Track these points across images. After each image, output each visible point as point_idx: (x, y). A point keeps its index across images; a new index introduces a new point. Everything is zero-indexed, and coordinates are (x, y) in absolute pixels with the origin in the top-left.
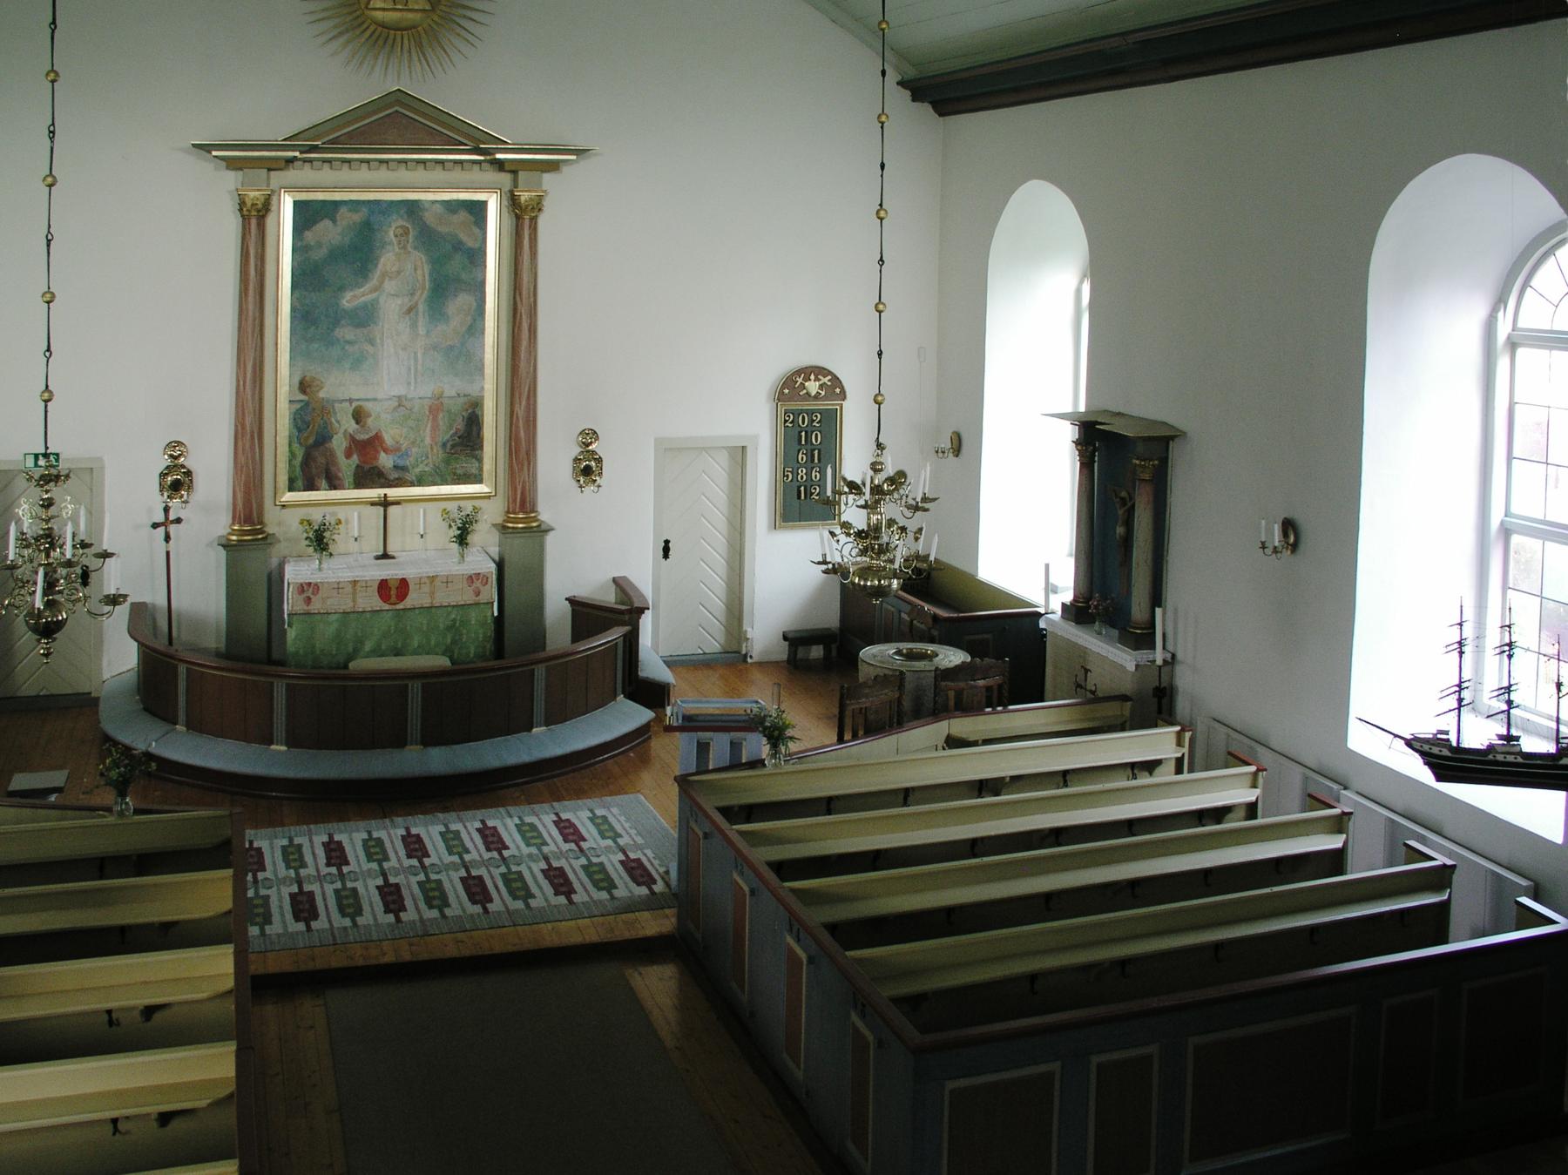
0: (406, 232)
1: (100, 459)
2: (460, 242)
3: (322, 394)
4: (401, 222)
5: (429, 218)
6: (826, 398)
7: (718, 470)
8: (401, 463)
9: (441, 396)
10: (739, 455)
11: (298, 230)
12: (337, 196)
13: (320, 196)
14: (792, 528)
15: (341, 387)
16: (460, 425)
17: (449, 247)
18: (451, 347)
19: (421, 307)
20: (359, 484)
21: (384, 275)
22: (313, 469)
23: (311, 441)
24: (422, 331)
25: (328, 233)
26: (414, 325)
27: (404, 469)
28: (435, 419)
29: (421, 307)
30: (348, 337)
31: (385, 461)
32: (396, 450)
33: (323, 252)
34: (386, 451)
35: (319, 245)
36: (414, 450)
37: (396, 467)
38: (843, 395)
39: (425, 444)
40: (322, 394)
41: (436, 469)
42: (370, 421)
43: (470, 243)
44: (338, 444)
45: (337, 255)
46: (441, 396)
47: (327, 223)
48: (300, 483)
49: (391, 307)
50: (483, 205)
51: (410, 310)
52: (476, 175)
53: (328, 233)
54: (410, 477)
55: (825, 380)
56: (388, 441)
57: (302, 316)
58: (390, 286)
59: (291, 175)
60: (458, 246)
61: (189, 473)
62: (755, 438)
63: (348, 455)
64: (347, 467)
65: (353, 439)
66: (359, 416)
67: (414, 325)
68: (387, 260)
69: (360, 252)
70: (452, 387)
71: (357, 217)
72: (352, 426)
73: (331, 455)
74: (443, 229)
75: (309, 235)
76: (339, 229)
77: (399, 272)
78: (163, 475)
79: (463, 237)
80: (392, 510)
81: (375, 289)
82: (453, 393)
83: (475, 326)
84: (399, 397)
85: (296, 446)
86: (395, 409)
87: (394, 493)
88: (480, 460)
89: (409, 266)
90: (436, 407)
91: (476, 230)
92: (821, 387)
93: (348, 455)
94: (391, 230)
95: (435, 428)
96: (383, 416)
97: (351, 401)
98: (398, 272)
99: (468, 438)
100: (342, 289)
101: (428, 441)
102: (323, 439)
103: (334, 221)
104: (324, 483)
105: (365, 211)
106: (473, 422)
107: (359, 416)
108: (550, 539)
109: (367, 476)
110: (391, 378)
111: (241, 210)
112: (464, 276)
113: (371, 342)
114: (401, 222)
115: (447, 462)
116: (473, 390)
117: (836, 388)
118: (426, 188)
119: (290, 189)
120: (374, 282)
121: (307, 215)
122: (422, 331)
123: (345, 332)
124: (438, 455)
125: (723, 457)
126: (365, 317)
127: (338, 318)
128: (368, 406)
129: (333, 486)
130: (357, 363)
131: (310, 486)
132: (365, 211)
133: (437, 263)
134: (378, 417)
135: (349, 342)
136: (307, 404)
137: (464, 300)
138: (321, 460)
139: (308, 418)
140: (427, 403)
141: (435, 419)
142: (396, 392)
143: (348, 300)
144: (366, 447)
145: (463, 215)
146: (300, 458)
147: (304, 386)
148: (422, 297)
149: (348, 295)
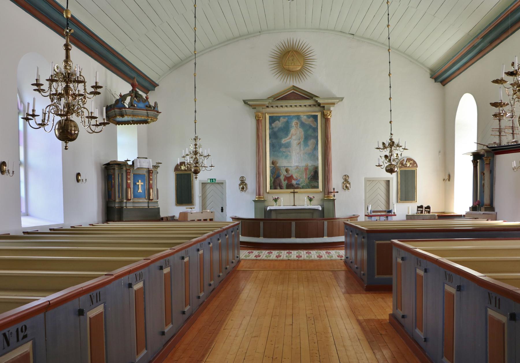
0: (297, 124)
1: (225, 181)
3: (278, 165)
8: (298, 183)
10: (388, 182)
11: (270, 124)
12: (279, 115)
13: (275, 115)
15: (283, 163)
16: (312, 173)
18: (309, 154)
19: (302, 143)
22: (276, 184)
24: (302, 149)
27: (299, 184)
28: (306, 172)
30: (284, 151)
31: (294, 182)
32: (297, 179)
34: (294, 180)
35: (276, 127)
37: (296, 184)
40: (278, 165)
41: (307, 185)
42: (290, 172)
43: (314, 126)
44: (282, 178)
45: (280, 129)
47: (277, 122)
48: (273, 187)
50: (317, 116)
51: (299, 144)
53: (278, 124)
54: (300, 186)
55: (411, 162)
56: (294, 177)
57: (272, 146)
58: (294, 137)
59: (271, 110)
60: (311, 127)
61: (246, 184)
62: (392, 178)
63: (285, 180)
64: (284, 183)
65: (285, 176)
66: (287, 171)
68: (293, 131)
69: (286, 129)
70: (310, 163)
71: (285, 120)
72: (285, 173)
73: (280, 180)
74: (307, 123)
75: (273, 125)
78: (240, 185)
79: (312, 125)
80: (296, 195)
81: (290, 138)
83: (316, 148)
84: (297, 166)
87: (296, 190)
88: (318, 182)
89: (298, 132)
90: (306, 169)
91: (315, 123)
92: (410, 164)
93: (285, 180)
94: (294, 122)
95: (306, 174)
98: (296, 134)
99: (315, 176)
100: (282, 138)
101: (304, 177)
102: (278, 176)
104: (279, 188)
105: (287, 118)
106: (316, 172)
107: (287, 171)
109: (290, 186)
110: (295, 161)
112: (312, 135)
113: (290, 152)
115: (309, 183)
116: (315, 164)
119: (268, 113)
120: (290, 136)
121: (273, 119)
122: (302, 149)
123: (283, 149)
124: (307, 181)
126: (288, 146)
127: (281, 146)
128: (289, 168)
129: (281, 188)
130: (286, 157)
131: (275, 188)
132: (287, 118)
133: (306, 131)
138: (278, 182)
140: (304, 167)
142: (296, 164)
143: (284, 141)
144: (289, 178)
145: (311, 119)
147: (273, 163)
148: (302, 141)
149: (283, 140)
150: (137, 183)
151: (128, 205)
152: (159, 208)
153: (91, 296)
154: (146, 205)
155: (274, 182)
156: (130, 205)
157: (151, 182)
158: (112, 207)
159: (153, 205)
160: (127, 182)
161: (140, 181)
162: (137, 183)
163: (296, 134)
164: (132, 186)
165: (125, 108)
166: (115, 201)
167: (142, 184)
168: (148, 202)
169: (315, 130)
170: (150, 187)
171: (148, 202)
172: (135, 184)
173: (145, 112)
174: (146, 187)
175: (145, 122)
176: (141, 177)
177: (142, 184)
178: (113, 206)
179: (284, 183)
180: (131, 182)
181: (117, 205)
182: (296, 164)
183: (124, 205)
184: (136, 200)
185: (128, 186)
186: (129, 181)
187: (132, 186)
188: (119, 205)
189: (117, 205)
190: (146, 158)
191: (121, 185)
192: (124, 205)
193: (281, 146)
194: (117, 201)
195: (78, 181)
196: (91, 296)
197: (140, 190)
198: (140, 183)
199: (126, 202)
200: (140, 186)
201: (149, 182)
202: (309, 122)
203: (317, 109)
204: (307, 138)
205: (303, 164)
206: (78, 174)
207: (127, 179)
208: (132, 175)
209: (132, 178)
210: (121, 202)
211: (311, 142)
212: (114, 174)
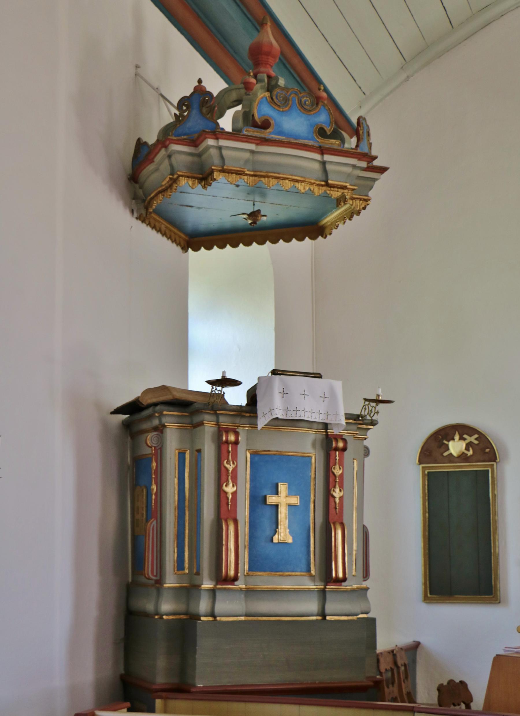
150: (272, 500)
151: (220, 607)
152: (372, 621)
154: (311, 606)
156: (230, 607)
157: (337, 493)
158: (146, 615)
159: (347, 607)
161: (283, 488)
162: (272, 500)
164: (243, 512)
165: (218, 133)
166: (159, 582)
167: (295, 500)
168: (323, 593)
170: (331, 517)
171: (323, 593)
172: (258, 501)
173: (309, 161)
174: (315, 516)
175: (310, 228)
177: (295, 500)
178: (150, 607)
180: (239, 489)
181: (167, 606)
183: (203, 606)
184: (264, 581)
185: (225, 511)
186: (230, 489)
187: (243, 512)
188: (181, 607)
189: (167, 606)
190: (318, 376)
191: (188, 506)
192: (203, 606)
194: (171, 581)
197: (284, 534)
198: (284, 499)
199: (213, 592)
200: (283, 513)
201: (328, 495)
208: (244, 455)
209: (245, 474)
210: (190, 590)
212: (160, 451)
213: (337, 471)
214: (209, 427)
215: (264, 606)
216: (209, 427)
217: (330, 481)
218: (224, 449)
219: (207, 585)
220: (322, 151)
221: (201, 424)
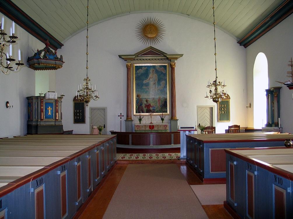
2: (162, 72)
3: (141, 97)
4: (152, 69)
5: (157, 68)
6: (226, 99)
7: (208, 112)
8: (154, 109)
9: (160, 98)
10: (212, 109)
11: (136, 71)
14: (221, 122)
15: (144, 96)
16: (163, 103)
17: (161, 73)
18: (162, 90)
20: (147, 112)
21: (150, 78)
23: (139, 105)
24: (156, 87)
25: (141, 71)
26: (155, 86)
27: (154, 110)
28: (159, 102)
29: (156, 83)
30: (145, 88)
31: (151, 108)
32: (153, 107)
33: (140, 74)
36: (156, 107)
37: (153, 110)
38: (230, 99)
39: (158, 106)
40: (141, 97)
42: (148, 102)
43: (164, 72)
44: (143, 106)
45: (142, 75)
46: (160, 98)
47: (140, 69)
49: (151, 83)
51: (155, 83)
52: (164, 61)
53: (141, 71)
54: (155, 111)
58: (151, 80)
60: (162, 73)
64: (145, 109)
66: (147, 101)
67: (155, 86)
68: (150, 75)
70: (162, 97)
71: (145, 68)
72: (146, 103)
73: (142, 107)
74: (159, 70)
76: (143, 70)
77: (152, 77)
79: (163, 71)
82: (162, 97)
85: (137, 106)
86: (153, 100)
91: (165, 71)
96: (151, 101)
97: (145, 98)
98: (152, 78)
100: (143, 80)
101: (158, 105)
102: (141, 105)
103: (142, 69)
107: (147, 101)
108: (178, 122)
110: (152, 95)
111: (127, 67)
112: (163, 78)
113: (148, 89)
114: (152, 69)
115: (161, 109)
117: (228, 97)
118: (156, 63)
120: (149, 79)
122: (156, 87)
123: (144, 87)
125: (209, 110)
126: (147, 85)
127: (143, 85)
130: (146, 92)
134: (150, 101)
135: (145, 89)
136: (138, 99)
137: (163, 82)
139: (139, 101)
141: (159, 102)
143: (144, 82)
144: (148, 106)
145: (163, 68)
146: (137, 107)
147: (138, 96)
153: (37, 180)
154: (54, 123)
155: (139, 108)
156: (42, 123)
158: (30, 125)
159: (58, 123)
160: (41, 108)
163: (152, 78)
164: (44, 111)
167: (51, 109)
169: (165, 75)
170: (57, 111)
172: (46, 109)
176: (51, 104)
177: (51, 109)
179: (145, 109)
182: (153, 97)
185: (42, 111)
186: (42, 108)
187: (44, 111)
188: (36, 124)
190: (54, 92)
192: (39, 123)
193: (143, 85)
194: (34, 120)
195: (7, 107)
196: (37, 180)
197: (50, 113)
198: (50, 109)
200: (50, 111)
201: (56, 108)
202: (162, 69)
203: (167, 61)
204: (159, 80)
205: (158, 97)
206: (7, 102)
207: (41, 106)
209: (44, 105)
211: (163, 82)
212: (32, 103)
213: (57, 105)
214: (39, 99)
215: (47, 123)
216: (39, 99)
217: (56, 106)
218: (41, 102)
219: (39, 120)
220: (55, 61)
221: (38, 99)
